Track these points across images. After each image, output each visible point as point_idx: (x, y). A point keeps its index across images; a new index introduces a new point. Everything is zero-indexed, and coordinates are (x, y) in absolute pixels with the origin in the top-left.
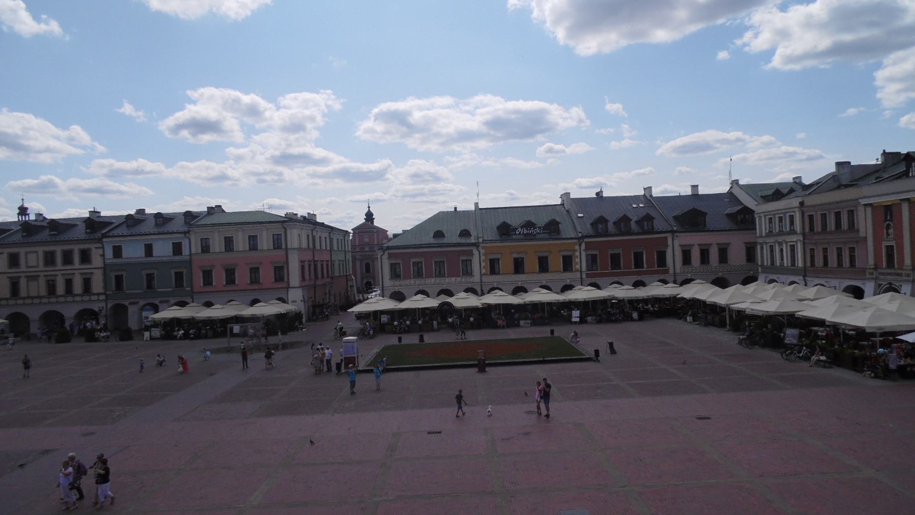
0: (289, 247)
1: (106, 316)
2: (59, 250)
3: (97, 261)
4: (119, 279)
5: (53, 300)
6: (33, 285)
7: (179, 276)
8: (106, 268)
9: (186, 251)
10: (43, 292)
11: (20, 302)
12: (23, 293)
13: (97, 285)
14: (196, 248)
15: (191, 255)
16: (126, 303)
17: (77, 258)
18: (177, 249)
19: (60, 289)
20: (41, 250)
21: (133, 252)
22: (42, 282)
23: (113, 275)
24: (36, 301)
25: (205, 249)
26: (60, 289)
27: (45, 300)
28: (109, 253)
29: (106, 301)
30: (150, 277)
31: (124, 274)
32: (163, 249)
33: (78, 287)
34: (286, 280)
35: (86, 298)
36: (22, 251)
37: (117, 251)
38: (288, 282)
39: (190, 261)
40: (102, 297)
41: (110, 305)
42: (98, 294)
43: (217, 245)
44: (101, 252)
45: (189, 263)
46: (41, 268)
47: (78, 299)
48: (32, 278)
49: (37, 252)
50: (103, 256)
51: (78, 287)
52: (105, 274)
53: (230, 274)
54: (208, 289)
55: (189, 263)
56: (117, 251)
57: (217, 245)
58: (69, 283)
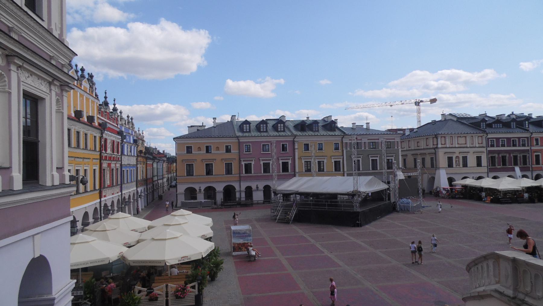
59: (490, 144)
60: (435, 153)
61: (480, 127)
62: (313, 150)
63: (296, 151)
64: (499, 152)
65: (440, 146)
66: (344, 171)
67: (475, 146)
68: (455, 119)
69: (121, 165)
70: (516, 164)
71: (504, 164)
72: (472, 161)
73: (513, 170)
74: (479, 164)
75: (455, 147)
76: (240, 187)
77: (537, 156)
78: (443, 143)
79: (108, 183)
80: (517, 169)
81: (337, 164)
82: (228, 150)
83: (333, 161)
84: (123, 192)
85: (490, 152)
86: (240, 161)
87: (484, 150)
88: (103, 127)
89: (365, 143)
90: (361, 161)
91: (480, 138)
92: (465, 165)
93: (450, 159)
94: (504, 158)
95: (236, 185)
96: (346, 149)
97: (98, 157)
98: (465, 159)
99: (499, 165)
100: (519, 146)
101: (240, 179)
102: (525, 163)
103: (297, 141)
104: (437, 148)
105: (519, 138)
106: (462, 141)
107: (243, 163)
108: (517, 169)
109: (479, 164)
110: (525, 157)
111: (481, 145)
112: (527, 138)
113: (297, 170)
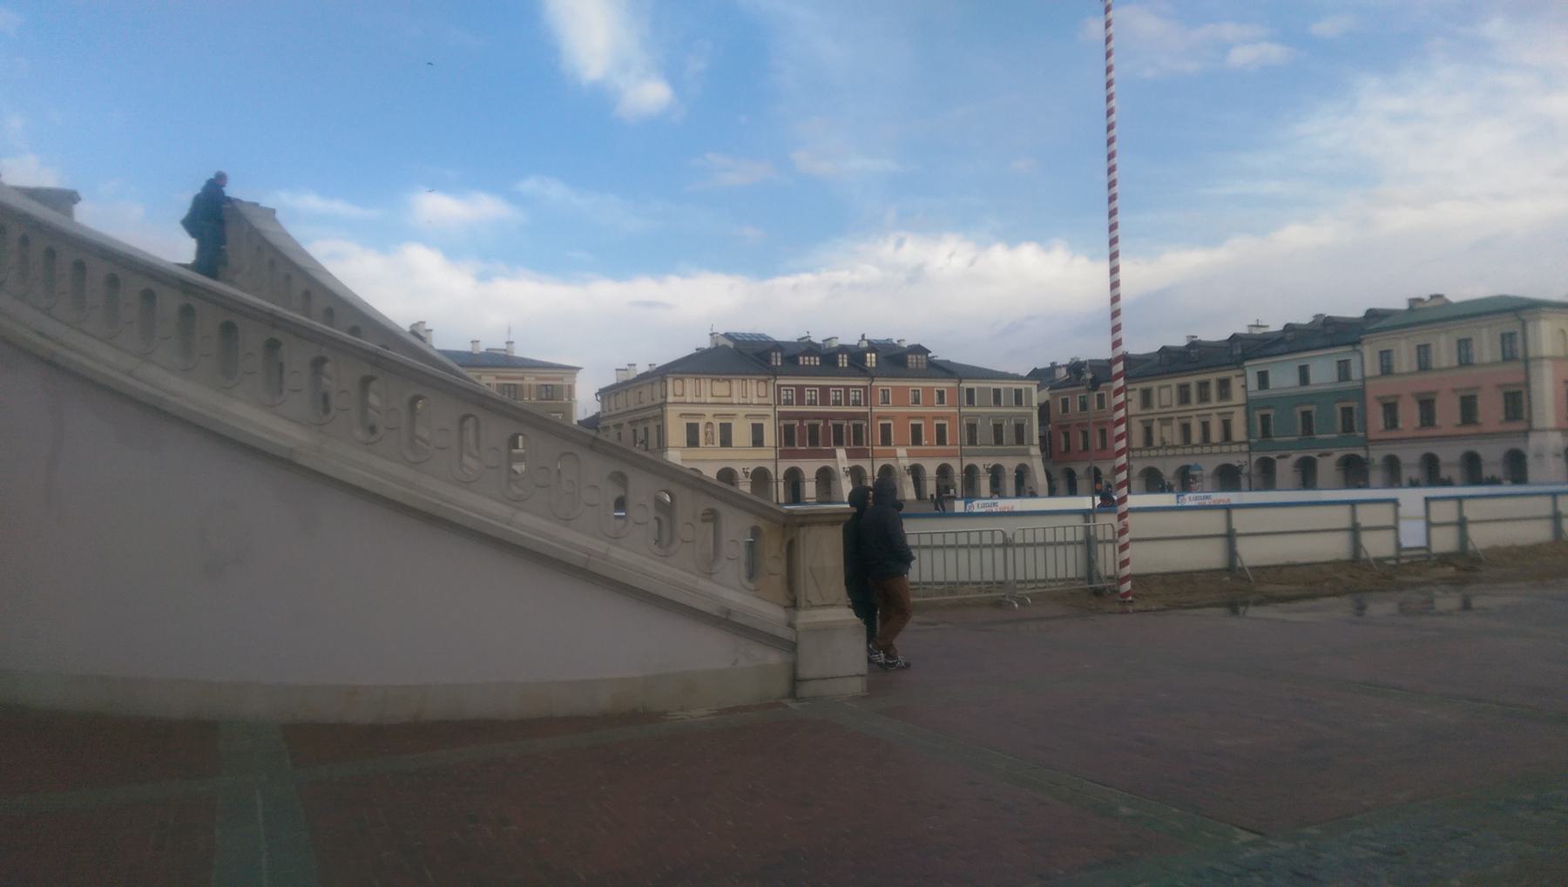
0: (1532, 353)
1: (1249, 475)
2: (1193, 380)
3: (1237, 396)
4: (1265, 418)
5: (1188, 451)
6: (1166, 429)
7: (1347, 412)
8: (1250, 406)
9: (1355, 374)
10: (1177, 440)
11: (1153, 453)
12: (1156, 442)
13: (1238, 432)
14: (1372, 367)
15: (1364, 379)
16: (1273, 456)
17: (1214, 391)
18: (1344, 369)
19: (1196, 436)
20: (1175, 382)
21: (1283, 376)
22: (1176, 424)
23: (1257, 415)
24: (1170, 452)
25: (1386, 370)
26: (1196, 436)
27: (1179, 451)
28: (1253, 383)
29: (1249, 452)
30: (1307, 416)
31: (1272, 412)
32: (1323, 371)
33: (1216, 434)
34: (1525, 415)
35: (1225, 449)
36: (1154, 385)
37: (1263, 378)
38: (1530, 421)
39: (1364, 387)
40: (1245, 448)
41: (1255, 457)
42: (1240, 443)
43: (1405, 359)
44: (1241, 381)
45: (1361, 393)
46: (1175, 407)
47: (1216, 449)
48: (1166, 421)
49: (1169, 386)
50: (1245, 386)
51: (1216, 434)
52: (1247, 413)
53: (1427, 406)
54: (1393, 434)
55: (1361, 393)
56: (1263, 378)
57: (1405, 359)
58: (1205, 426)
59: (783, 397)
60: (661, 417)
61: (768, 361)
64: (801, 417)
65: (670, 399)
67: (750, 400)
68: (731, 344)
70: (839, 442)
71: (814, 440)
72: (742, 433)
73: (833, 455)
74: (758, 441)
75: (705, 403)
77: (886, 429)
78: (679, 392)
80: (841, 453)
85: (783, 416)
87: (770, 411)
91: (762, 385)
92: (726, 441)
93: (692, 430)
94: (813, 428)
98: (726, 430)
99: (802, 443)
100: (847, 404)
102: (858, 439)
104: (666, 403)
105: (847, 388)
106: (721, 388)
108: (841, 453)
109: (758, 441)
110: (858, 430)
111: (765, 401)
112: (865, 388)
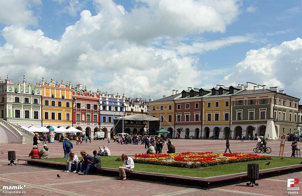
62: (213, 106)
63: (203, 107)
66: (230, 120)
69: (100, 115)
76: (175, 129)
79: (83, 119)
81: (227, 115)
82: (170, 108)
83: (224, 114)
84: (101, 126)
86: (175, 114)
88: (74, 99)
89: (246, 100)
90: (285, 114)
95: (173, 127)
96: (233, 105)
97: (72, 110)
101: (175, 124)
103: (204, 101)
107: (177, 115)
113: (203, 120)
